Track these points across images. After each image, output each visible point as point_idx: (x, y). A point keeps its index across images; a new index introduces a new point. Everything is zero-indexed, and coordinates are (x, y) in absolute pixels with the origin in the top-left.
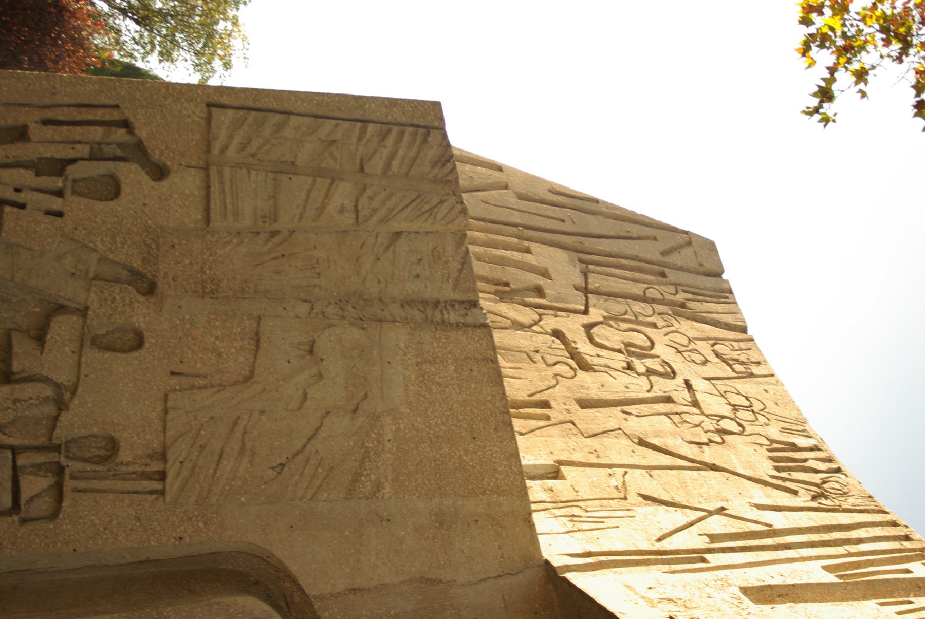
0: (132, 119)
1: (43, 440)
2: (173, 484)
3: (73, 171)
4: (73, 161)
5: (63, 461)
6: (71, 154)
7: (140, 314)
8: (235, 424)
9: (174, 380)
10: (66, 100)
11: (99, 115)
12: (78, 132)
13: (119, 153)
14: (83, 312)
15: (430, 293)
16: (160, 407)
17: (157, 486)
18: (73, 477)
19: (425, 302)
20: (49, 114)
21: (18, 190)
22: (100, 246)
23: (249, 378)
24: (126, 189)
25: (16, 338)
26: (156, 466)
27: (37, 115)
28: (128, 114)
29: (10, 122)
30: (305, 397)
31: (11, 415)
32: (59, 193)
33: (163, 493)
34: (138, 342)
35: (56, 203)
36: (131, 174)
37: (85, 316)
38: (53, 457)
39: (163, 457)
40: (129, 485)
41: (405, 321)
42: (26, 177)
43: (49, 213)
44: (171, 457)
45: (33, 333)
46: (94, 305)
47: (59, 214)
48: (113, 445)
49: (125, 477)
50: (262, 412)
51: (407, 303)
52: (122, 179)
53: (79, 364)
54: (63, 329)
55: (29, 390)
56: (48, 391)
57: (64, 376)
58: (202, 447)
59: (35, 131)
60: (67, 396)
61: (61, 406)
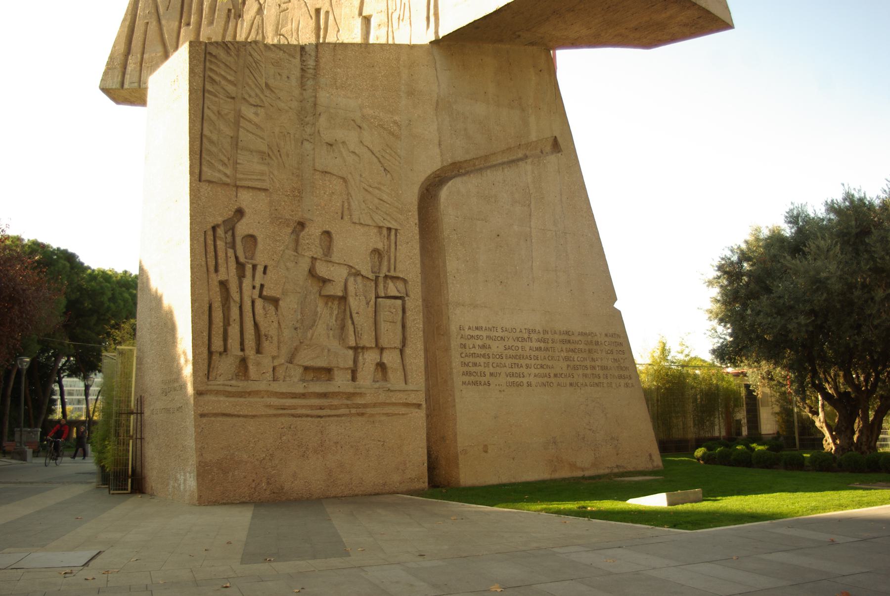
0: (212, 225)
1: (373, 284)
2: (393, 225)
3: (242, 259)
4: (237, 258)
5: (382, 275)
6: (233, 259)
7: (313, 231)
8: (366, 190)
9: (346, 218)
10: (204, 259)
11: (210, 242)
12: (221, 254)
13: (230, 233)
14: (314, 259)
16: (358, 227)
17: (393, 232)
18: (389, 271)
20: (212, 269)
21: (254, 287)
22: (281, 248)
23: (344, 180)
24: (251, 232)
25: (324, 293)
26: (385, 232)
27: (213, 275)
28: (209, 226)
29: (218, 289)
30: (354, 153)
31: (362, 298)
32: (254, 267)
33: (396, 230)
34: (327, 233)
35: (260, 269)
36: (242, 228)
37: (316, 259)
38: (381, 280)
39: (380, 227)
40: (393, 246)
42: (247, 283)
43: (265, 272)
44: (381, 225)
45: (321, 285)
46: (311, 254)
47: (265, 268)
48: (376, 251)
49: (390, 247)
50: (361, 176)
52: (246, 233)
53: (339, 264)
54: (322, 270)
55: (351, 289)
56: (352, 279)
57: (344, 272)
58: (377, 208)
59: (222, 276)
60: (353, 271)
61: (358, 274)
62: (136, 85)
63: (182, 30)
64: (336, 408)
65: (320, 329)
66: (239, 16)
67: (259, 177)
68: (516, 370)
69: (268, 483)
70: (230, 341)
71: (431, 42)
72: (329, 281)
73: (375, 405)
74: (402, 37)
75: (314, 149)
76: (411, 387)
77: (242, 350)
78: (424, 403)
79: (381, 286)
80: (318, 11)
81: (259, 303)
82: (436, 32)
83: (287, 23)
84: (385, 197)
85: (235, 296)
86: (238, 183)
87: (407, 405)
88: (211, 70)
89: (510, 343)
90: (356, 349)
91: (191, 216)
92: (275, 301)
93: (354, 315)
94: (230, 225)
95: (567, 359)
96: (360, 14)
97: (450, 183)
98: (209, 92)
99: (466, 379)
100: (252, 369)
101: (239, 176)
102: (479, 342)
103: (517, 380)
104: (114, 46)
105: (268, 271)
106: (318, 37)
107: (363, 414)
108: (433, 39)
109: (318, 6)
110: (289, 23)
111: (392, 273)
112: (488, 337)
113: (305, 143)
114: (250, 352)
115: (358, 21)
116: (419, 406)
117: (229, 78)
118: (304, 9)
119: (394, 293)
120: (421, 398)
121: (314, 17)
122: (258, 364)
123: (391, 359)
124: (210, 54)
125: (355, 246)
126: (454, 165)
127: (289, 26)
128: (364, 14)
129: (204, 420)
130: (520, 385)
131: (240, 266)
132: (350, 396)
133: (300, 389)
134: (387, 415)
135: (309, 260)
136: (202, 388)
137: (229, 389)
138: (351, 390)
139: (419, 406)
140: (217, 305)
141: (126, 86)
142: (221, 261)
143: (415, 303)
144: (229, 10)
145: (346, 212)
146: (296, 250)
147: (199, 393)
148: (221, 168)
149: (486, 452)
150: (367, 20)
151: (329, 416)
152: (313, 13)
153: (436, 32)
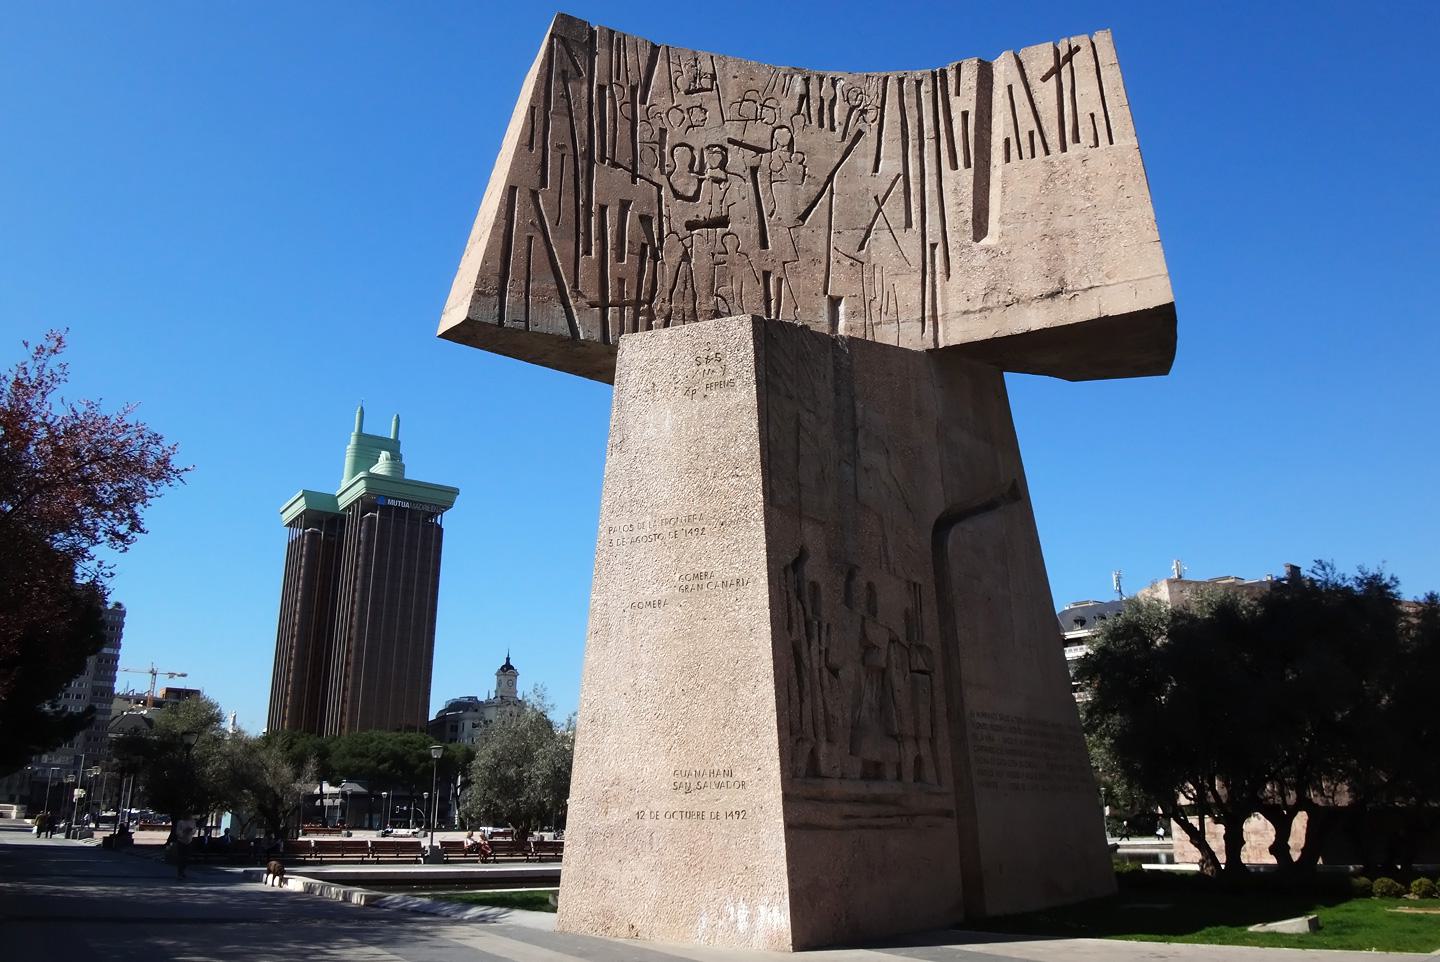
7: (861, 580)
34: (870, 586)
63: (582, 259)
74: (886, 335)
80: (767, 275)
82: (936, 340)
85: (806, 662)
90: (894, 737)
93: (896, 694)
104: (485, 261)
106: (768, 310)
116: (948, 814)
119: (923, 667)
121: (761, 281)
125: (892, 598)
127: (729, 287)
131: (808, 624)
139: (948, 814)
140: (793, 672)
141: (507, 323)
142: (794, 614)
152: (760, 275)
153: (936, 340)
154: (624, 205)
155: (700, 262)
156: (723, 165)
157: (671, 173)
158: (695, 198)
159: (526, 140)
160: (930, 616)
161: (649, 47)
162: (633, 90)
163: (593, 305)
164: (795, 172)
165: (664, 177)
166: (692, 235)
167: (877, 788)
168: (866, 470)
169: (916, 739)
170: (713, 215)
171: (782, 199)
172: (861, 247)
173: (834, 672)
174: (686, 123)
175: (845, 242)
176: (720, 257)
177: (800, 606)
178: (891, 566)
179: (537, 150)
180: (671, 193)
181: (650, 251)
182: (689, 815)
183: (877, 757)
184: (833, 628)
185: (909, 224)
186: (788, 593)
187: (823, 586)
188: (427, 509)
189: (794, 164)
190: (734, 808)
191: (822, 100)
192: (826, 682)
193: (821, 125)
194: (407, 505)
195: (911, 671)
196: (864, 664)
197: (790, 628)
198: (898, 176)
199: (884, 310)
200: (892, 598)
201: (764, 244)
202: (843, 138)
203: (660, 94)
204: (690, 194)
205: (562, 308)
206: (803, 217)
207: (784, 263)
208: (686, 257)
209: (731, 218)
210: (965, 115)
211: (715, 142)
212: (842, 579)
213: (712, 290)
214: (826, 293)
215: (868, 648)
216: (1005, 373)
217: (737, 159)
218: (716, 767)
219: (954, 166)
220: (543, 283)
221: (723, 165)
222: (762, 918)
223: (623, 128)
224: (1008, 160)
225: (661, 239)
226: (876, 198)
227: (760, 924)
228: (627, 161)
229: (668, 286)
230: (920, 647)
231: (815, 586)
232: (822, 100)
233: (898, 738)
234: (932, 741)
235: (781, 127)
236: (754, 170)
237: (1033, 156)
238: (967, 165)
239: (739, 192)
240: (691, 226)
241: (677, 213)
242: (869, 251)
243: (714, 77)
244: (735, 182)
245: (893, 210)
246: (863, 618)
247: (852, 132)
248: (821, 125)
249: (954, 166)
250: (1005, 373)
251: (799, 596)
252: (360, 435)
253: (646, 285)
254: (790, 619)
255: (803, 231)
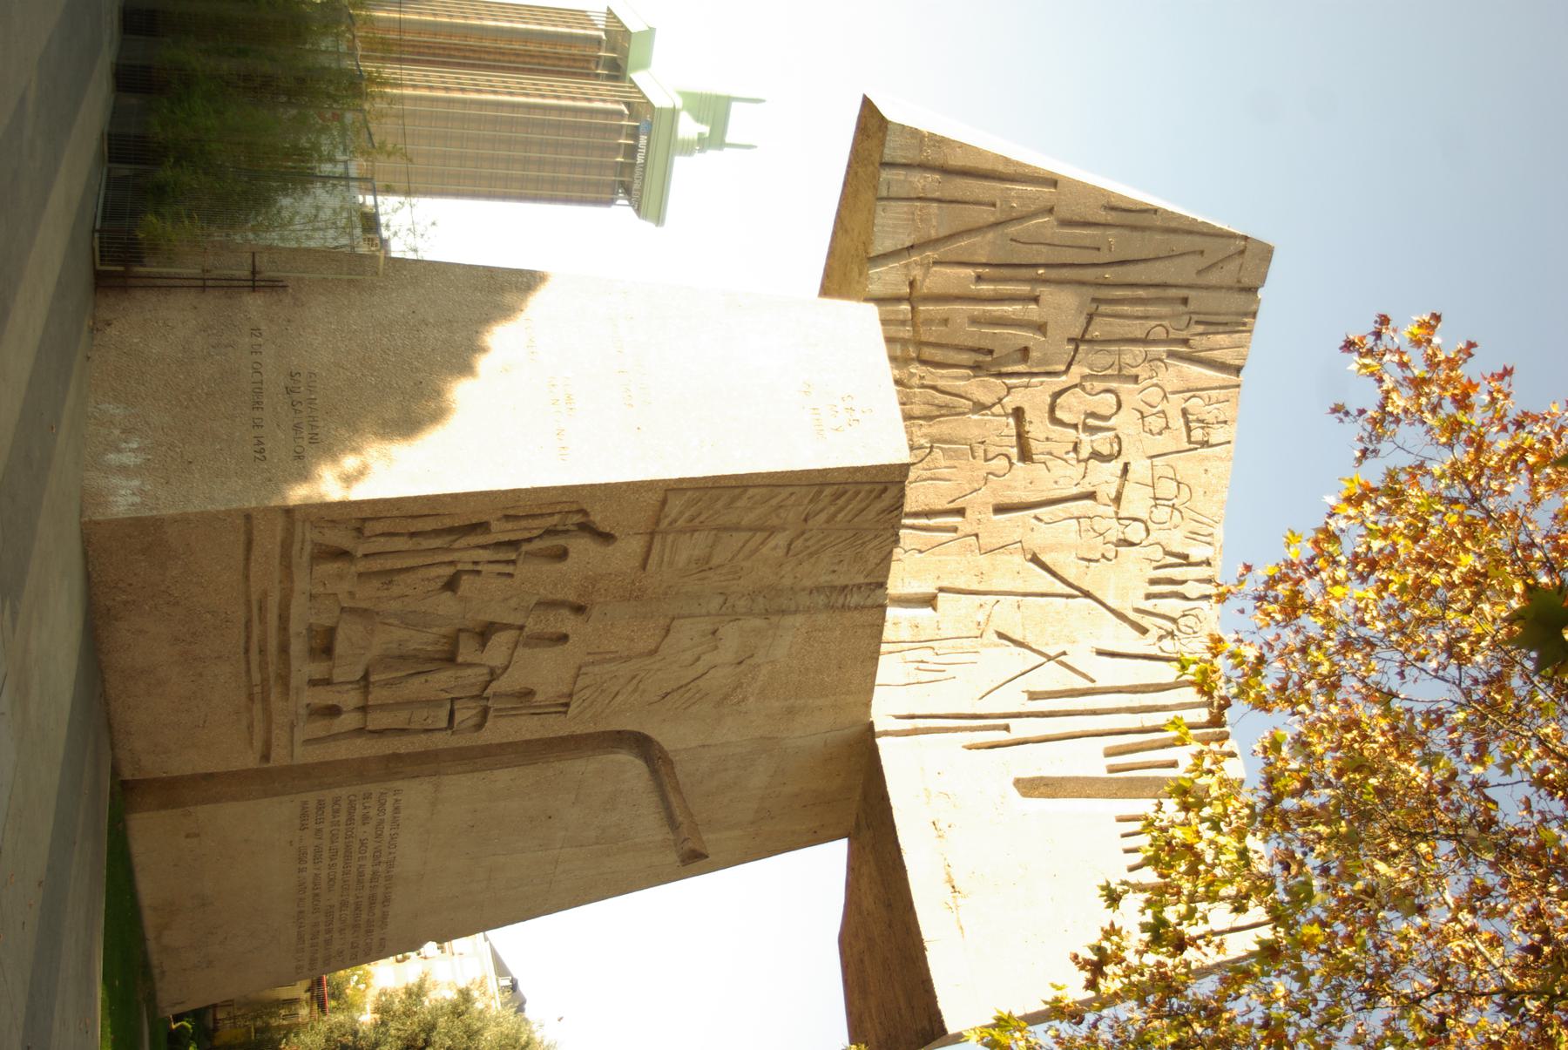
3: (525, 547)
5: (490, 704)
6: (527, 535)
7: (567, 622)
9: (590, 659)
15: (841, 581)
16: (573, 672)
19: (833, 588)
25: (463, 636)
30: (698, 659)
32: (513, 562)
34: (564, 638)
38: (483, 703)
39: (571, 695)
41: (808, 610)
51: (818, 589)
54: (501, 641)
56: (485, 671)
59: (495, 526)
61: (493, 675)
62: (884, 194)
64: (263, 666)
65: (400, 633)
66: (977, 368)
67: (666, 559)
68: (326, 854)
69: (125, 603)
70: (383, 539)
71: (871, 724)
72: (484, 645)
73: (267, 711)
74: (889, 668)
75: (709, 614)
76: (298, 750)
77: (366, 556)
78: (271, 764)
79: (472, 704)
80: (960, 512)
81: (450, 570)
82: (886, 733)
83: (951, 458)
84: (620, 698)
85: (462, 542)
86: (658, 539)
87: (268, 745)
88: (857, 493)
89: (371, 845)
90: (366, 677)
91: (606, 485)
92: (451, 585)
93: (422, 678)
94: (587, 528)
95: (344, 904)
96: (941, 590)
97: (639, 763)
98: (821, 492)
99: (312, 805)
100: (332, 567)
101: (670, 538)
102: (373, 812)
103: (310, 857)
104: (962, 145)
105: (503, 579)
106: (916, 515)
107: (251, 697)
108: (877, 729)
109: (968, 513)
110: (949, 463)
111: (491, 713)
112: (382, 821)
113: (721, 599)
114: (362, 566)
115: (928, 588)
116: (266, 757)
117: (840, 516)
118: (967, 488)
119: (458, 717)
120: (279, 758)
121: (952, 506)
122: (341, 577)
123: (349, 721)
124: (885, 490)
125: (544, 671)
126: (669, 762)
127: (943, 463)
128: (941, 595)
129: (240, 522)
130: (301, 859)
131: (513, 544)
132: (284, 679)
133: (296, 626)
134: (250, 726)
135: (520, 623)
136: (297, 515)
137: (296, 547)
138: (294, 682)
139: (266, 757)
140: (448, 523)
141: (886, 175)
142: (524, 523)
143: (442, 741)
144: (991, 352)
145: (598, 657)
146: (539, 604)
147: (289, 512)
148: (687, 515)
149: (187, 836)
150: (929, 601)
151: (248, 662)
153: (886, 733)
154: (1041, 328)
155: (972, 426)
156: (1096, 455)
157: (1083, 389)
158: (1055, 421)
159: (1114, 202)
160: (528, 728)
161: (1237, 362)
162: (1185, 342)
163: (912, 284)
164: (1091, 549)
165: (1078, 381)
166: (1007, 415)
167: (297, 647)
168: (714, 633)
169: (363, 709)
170: (1033, 443)
171: (1057, 534)
172: (1001, 636)
173: (451, 585)
174: (1147, 410)
175: (1007, 615)
176: (980, 453)
177: (536, 533)
178: (590, 669)
179: (1103, 216)
180: (1057, 389)
181: (984, 362)
182: (258, 391)
183: (340, 647)
184: (509, 581)
185: (1033, 696)
186: (552, 514)
187: (562, 566)
188: (636, 186)
189: (1102, 549)
190: (268, 445)
191: (1183, 582)
192: (434, 572)
193: (1153, 582)
194: (640, 159)
195: (453, 700)
196: (460, 630)
197: (507, 517)
198: (1093, 681)
199: (922, 666)
200: (544, 671)
201: (1000, 509)
202: (1138, 610)
203: (1180, 376)
204: (1059, 414)
205: (908, 244)
206: (1035, 560)
207: (977, 536)
208: (980, 407)
209: (1029, 466)
210: (1174, 764)
211: (1124, 445)
212: (572, 597)
213: (938, 441)
214: (941, 590)
215: (485, 633)
216: (845, 841)
217: (1104, 476)
218: (321, 424)
219: (1109, 753)
220: (937, 221)
221: (1096, 455)
222: (124, 483)
223: (1137, 329)
224: (1121, 820)
225: (1000, 375)
226: (1064, 653)
227: (115, 481)
228: (1095, 333)
229: (941, 383)
230: (485, 712)
231: (562, 555)
232: (1183, 582)
233: (365, 682)
234: (361, 731)
235: (1148, 530)
236: (1091, 496)
237: (1127, 851)
238: (1112, 770)
239: (1062, 476)
240: (1018, 413)
241: (1033, 396)
242: (997, 646)
243: (1205, 444)
244: (1076, 471)
245: (1052, 677)
246: (521, 628)
247: (1146, 621)
248: (1153, 582)
249: (1109, 753)
250: (845, 841)
251: (550, 532)
252: (729, 100)
253: (939, 355)
254: (516, 518)
255: (1018, 560)
